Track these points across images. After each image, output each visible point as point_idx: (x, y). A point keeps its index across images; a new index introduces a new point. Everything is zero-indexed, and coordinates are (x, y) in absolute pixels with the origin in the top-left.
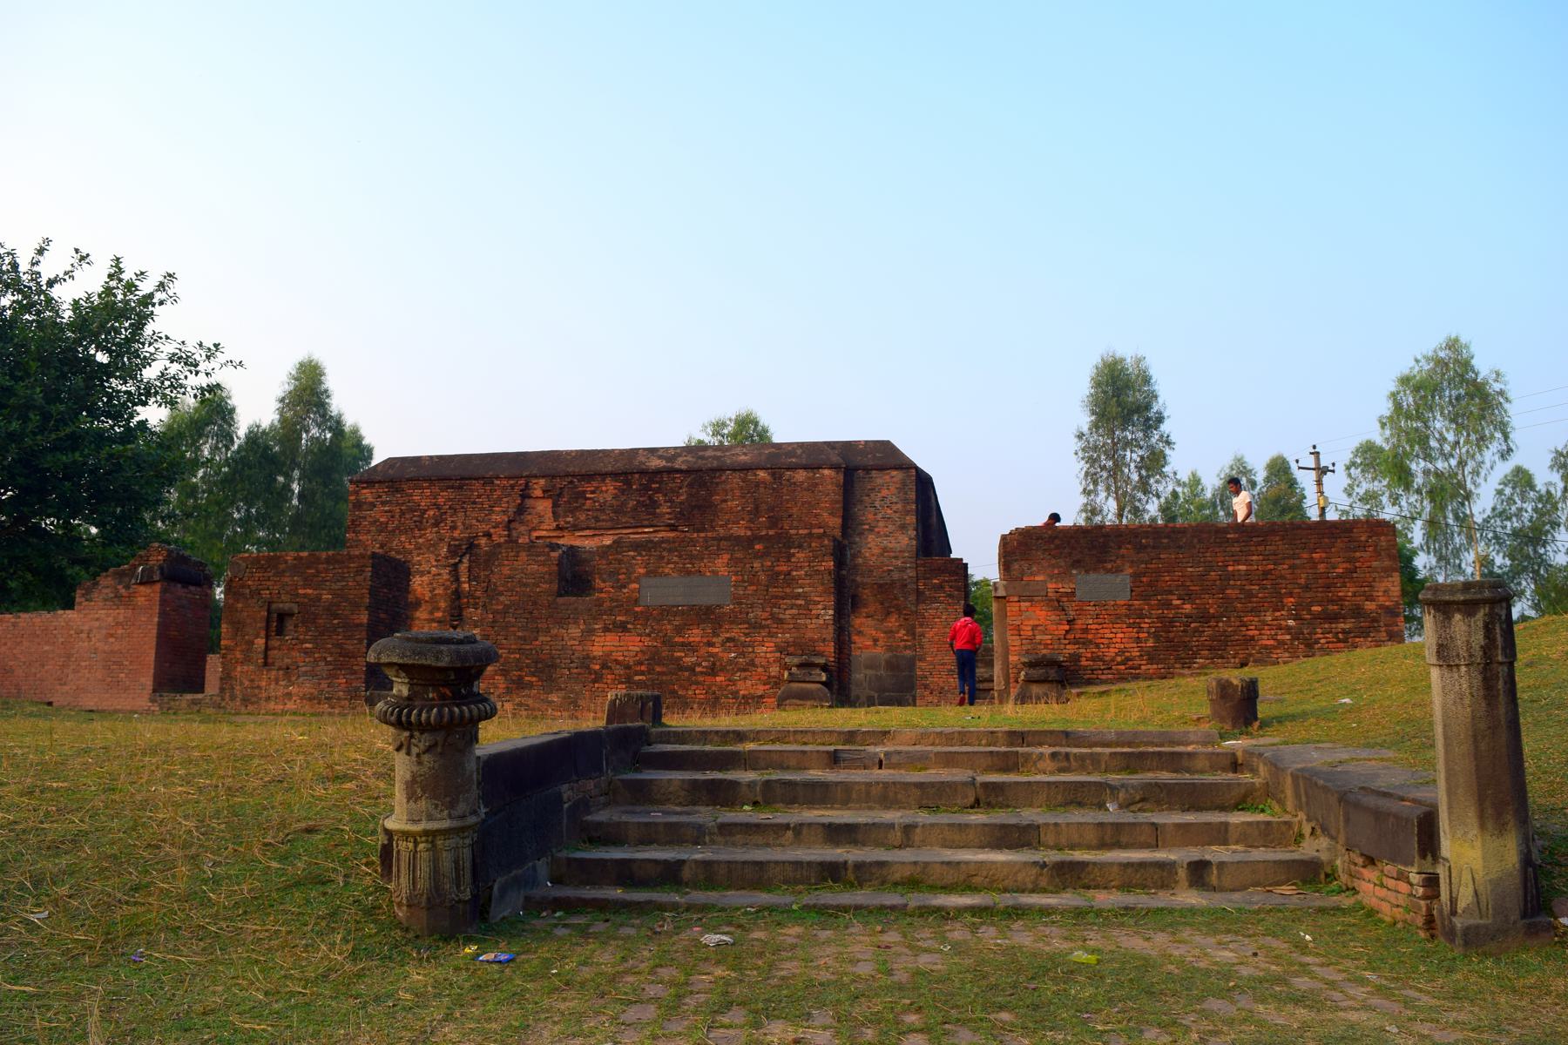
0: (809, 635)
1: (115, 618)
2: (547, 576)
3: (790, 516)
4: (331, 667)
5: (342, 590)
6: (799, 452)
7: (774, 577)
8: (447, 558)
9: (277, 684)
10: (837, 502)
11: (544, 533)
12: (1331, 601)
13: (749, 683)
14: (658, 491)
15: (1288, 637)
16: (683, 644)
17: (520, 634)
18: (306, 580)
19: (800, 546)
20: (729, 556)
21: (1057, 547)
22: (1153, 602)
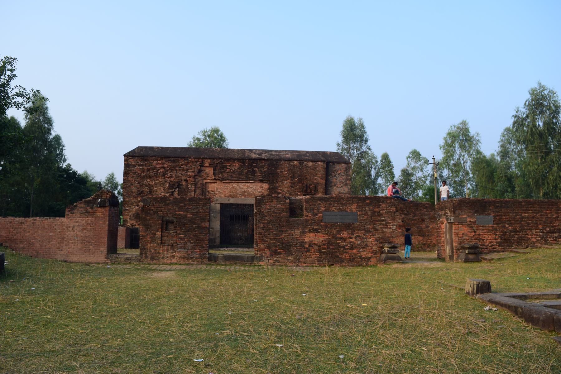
0: (387, 235)
1: (86, 222)
2: (285, 210)
3: (306, 179)
4: (193, 245)
5: (197, 212)
6: (308, 155)
7: (374, 213)
8: (169, 189)
9: (168, 251)
10: (324, 174)
11: (209, 181)
12: (552, 227)
13: (365, 253)
14: (256, 166)
15: (540, 238)
16: (340, 238)
17: (275, 232)
18: (179, 208)
19: (383, 202)
20: (357, 205)
21: (470, 206)
22: (500, 226)
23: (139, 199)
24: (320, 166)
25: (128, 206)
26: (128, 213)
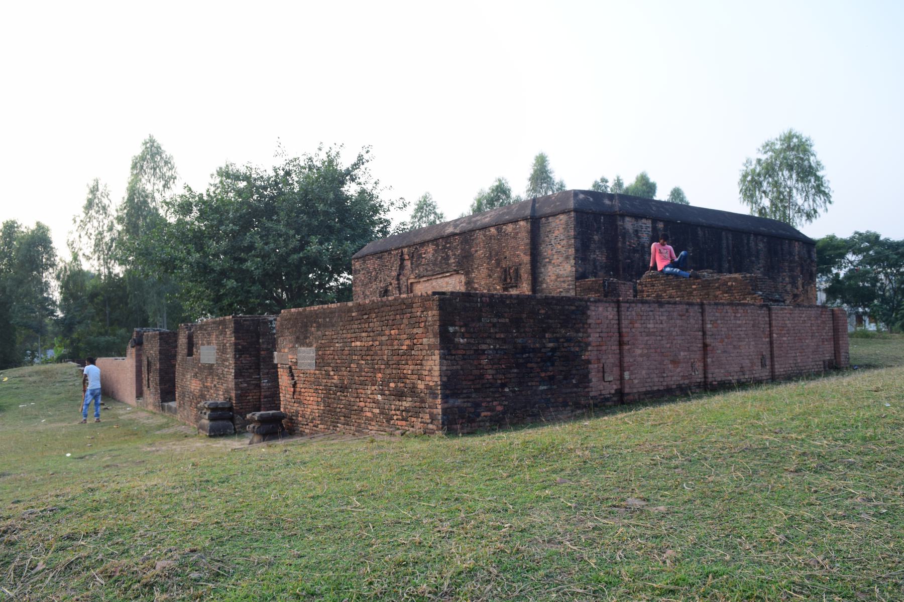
14: (449, 248)
24: (523, 229)
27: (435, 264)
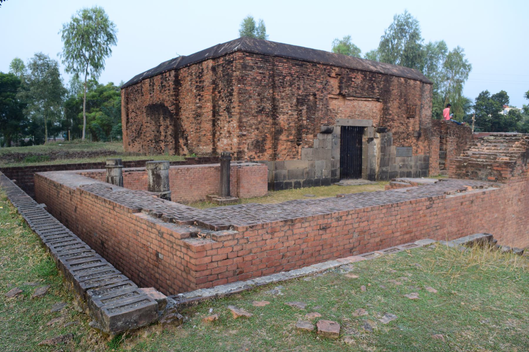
11: (332, 96)
14: (374, 81)
23: (259, 120)
24: (418, 86)
25: (245, 129)
26: (246, 140)
27: (363, 89)
